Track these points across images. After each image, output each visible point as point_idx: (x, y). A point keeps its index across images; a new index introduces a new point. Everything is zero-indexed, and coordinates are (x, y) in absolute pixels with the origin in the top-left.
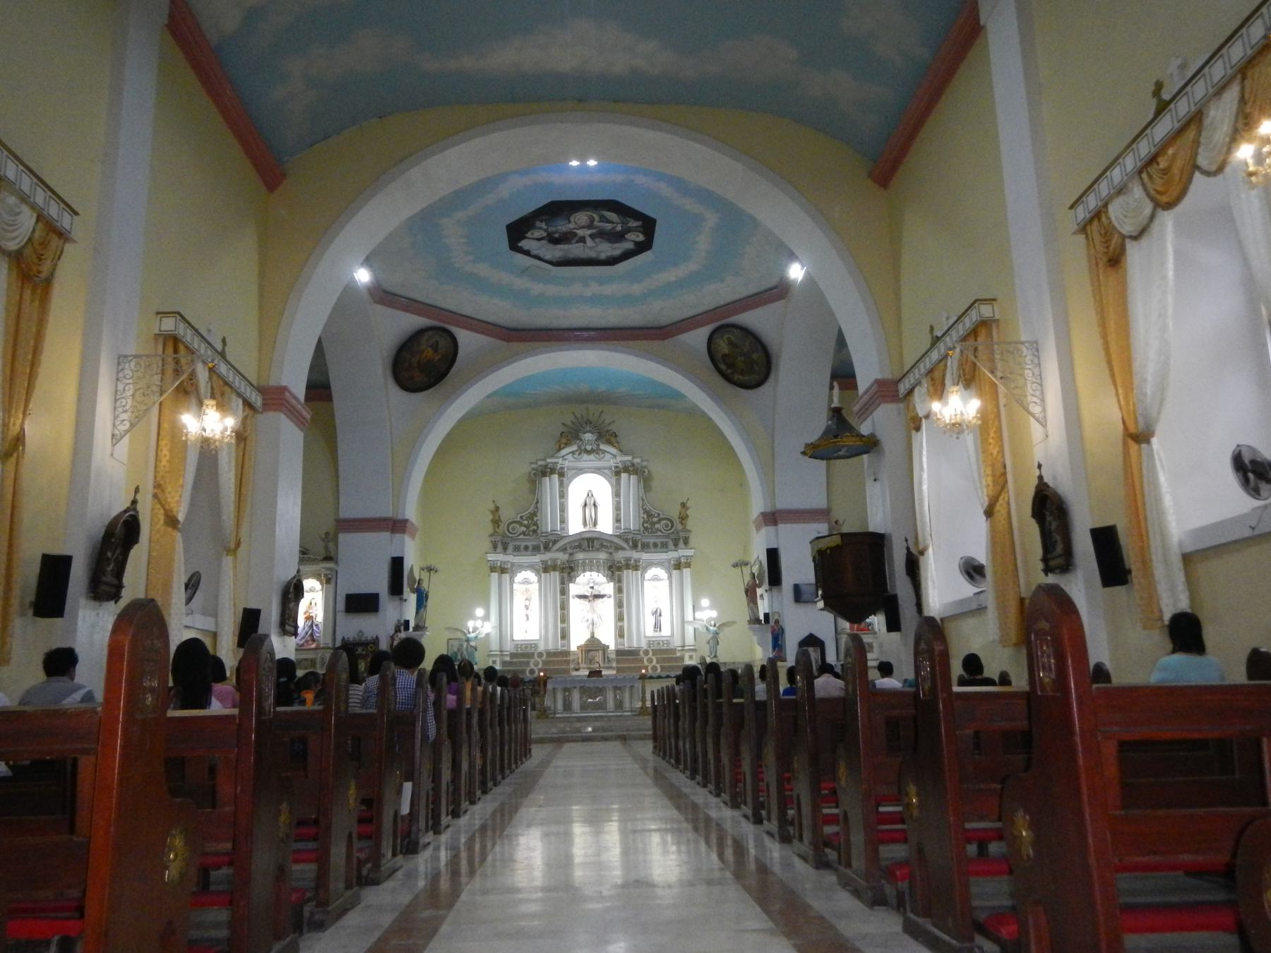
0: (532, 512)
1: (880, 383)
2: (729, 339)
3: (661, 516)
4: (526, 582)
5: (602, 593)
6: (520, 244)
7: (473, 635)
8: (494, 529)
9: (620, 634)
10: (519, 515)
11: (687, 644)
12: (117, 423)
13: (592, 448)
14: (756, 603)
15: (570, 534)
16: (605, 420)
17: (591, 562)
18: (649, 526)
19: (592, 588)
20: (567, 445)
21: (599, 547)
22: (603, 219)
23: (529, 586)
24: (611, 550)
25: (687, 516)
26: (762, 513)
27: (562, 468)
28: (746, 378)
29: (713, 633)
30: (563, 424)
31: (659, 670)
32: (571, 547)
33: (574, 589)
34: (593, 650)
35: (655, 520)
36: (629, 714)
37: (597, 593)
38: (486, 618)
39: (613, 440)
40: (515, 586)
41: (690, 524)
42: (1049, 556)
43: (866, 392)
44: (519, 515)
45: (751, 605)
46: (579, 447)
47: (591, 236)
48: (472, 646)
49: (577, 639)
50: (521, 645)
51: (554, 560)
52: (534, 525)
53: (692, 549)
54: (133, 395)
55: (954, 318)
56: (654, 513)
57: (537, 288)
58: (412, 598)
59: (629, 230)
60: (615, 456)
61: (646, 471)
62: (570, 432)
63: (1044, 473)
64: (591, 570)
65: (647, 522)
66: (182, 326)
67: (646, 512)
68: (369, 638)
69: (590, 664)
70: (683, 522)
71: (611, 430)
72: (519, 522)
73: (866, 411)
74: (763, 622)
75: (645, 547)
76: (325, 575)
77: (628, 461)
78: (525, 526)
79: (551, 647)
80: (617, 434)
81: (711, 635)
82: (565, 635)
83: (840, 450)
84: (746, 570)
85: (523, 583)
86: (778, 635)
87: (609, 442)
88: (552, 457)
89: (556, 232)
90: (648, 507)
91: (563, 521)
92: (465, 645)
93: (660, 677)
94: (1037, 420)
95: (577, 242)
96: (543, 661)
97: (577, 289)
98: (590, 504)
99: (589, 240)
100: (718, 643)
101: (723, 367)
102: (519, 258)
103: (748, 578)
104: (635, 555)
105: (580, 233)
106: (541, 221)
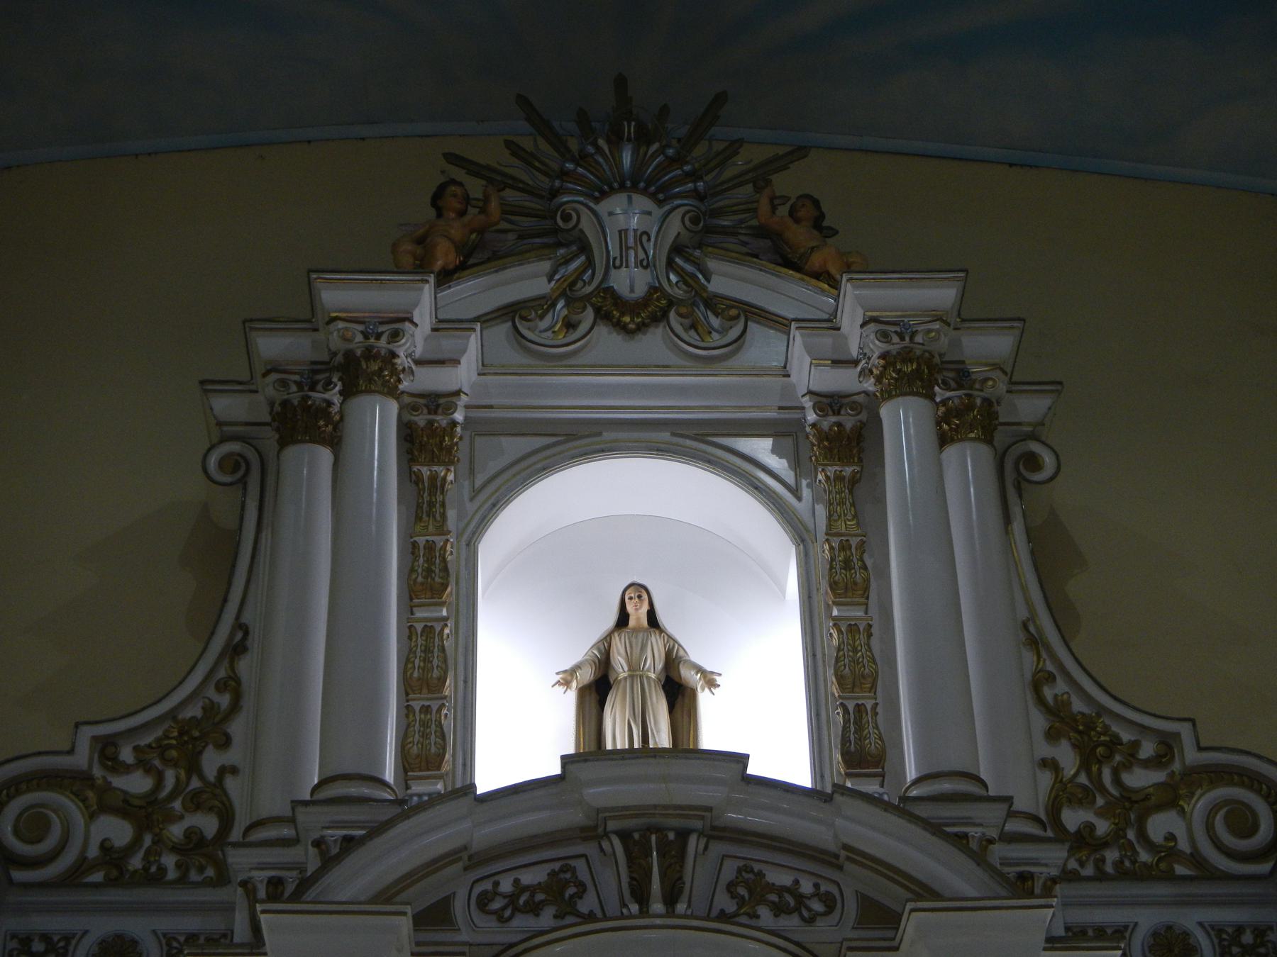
0: (194, 711)
3: (1192, 756)
13: (654, 289)
15: (487, 779)
21: (724, 902)
27: (438, 402)
30: (454, 159)
32: (483, 902)
35: (1139, 779)
39: (800, 235)
44: (87, 732)
52: (196, 803)
56: (1126, 736)
61: (1048, 459)
62: (509, 211)
65: (1083, 798)
71: (785, 199)
72: (85, 778)
78: (125, 807)
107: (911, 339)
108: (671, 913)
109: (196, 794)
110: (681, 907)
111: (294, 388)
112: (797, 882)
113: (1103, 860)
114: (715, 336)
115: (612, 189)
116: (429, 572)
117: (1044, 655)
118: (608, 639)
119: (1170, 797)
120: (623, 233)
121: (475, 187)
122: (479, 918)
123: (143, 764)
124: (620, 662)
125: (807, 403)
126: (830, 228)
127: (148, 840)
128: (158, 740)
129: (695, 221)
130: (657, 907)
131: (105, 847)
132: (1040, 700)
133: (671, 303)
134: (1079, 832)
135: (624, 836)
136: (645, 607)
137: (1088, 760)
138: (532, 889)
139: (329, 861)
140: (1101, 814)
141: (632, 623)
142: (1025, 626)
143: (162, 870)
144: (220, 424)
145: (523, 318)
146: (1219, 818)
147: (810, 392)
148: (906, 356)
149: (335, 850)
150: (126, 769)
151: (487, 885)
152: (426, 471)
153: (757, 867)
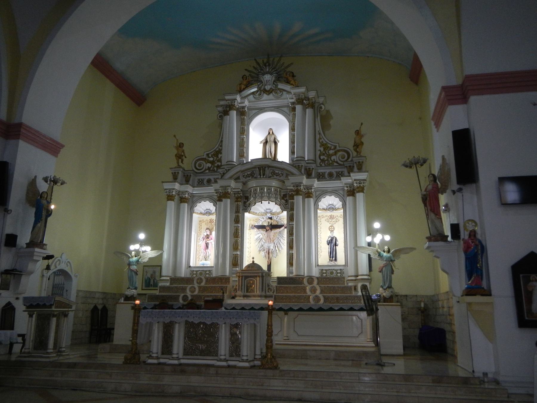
0: (217, 150)
3: (338, 148)
5: (280, 224)
7: (135, 259)
8: (178, 163)
11: (360, 274)
14: (438, 214)
16: (284, 63)
17: (262, 189)
18: (326, 158)
19: (271, 218)
20: (248, 85)
21: (270, 175)
24: (282, 178)
25: (362, 143)
26: (444, 88)
29: (385, 261)
30: (246, 70)
31: (322, 301)
32: (244, 176)
33: (249, 218)
34: (251, 277)
35: (331, 152)
36: (246, 364)
37: (274, 223)
39: (290, 78)
40: (195, 216)
41: (365, 150)
44: (205, 153)
45: (432, 215)
48: (132, 271)
50: (197, 271)
56: (329, 146)
60: (290, 93)
65: (324, 155)
67: (322, 145)
69: (247, 292)
70: (358, 149)
72: (206, 159)
74: (449, 239)
75: (320, 177)
77: (304, 93)
80: (294, 75)
81: (382, 263)
84: (423, 171)
85: (204, 214)
86: (476, 255)
93: (321, 309)
103: (426, 183)
107: (299, 96)
108: (263, 177)
109: (218, 160)
110: (264, 176)
111: (225, 108)
112: (279, 172)
113: (325, 163)
114: (279, 94)
115: (265, 74)
116: (242, 131)
117: (321, 135)
118: (267, 136)
119: (335, 154)
120: (266, 81)
121: (247, 74)
122: (243, 178)
123: (212, 157)
124: (268, 139)
125: (290, 104)
126: (295, 76)
127: (213, 166)
128: (214, 154)
129: (276, 77)
130: (262, 176)
131: (208, 167)
132: (319, 142)
133: (273, 90)
134: (323, 159)
135: (258, 168)
136: (272, 131)
137: (324, 149)
138: (249, 174)
139: (227, 172)
140: (325, 156)
141: (270, 134)
142: (319, 131)
143: (215, 170)
144: (219, 111)
145: (254, 94)
146: (340, 156)
147: (290, 102)
148: (299, 99)
149: (228, 170)
150: (210, 157)
151: (244, 174)
152: (242, 117)
153: (275, 171)
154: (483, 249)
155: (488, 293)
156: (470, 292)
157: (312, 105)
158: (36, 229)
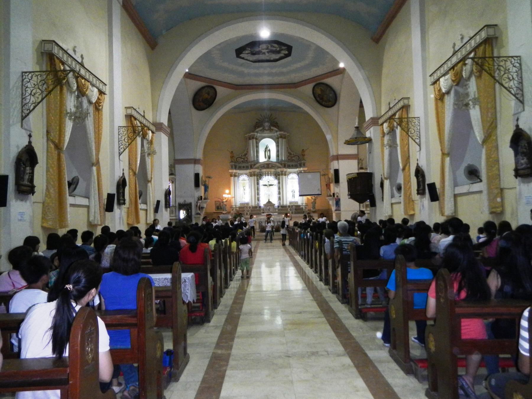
1: (372, 119)
2: (321, 88)
3: (295, 155)
4: (244, 180)
5: (272, 184)
6: (240, 56)
9: (279, 198)
10: (240, 155)
12: (120, 149)
19: (269, 182)
20: (259, 127)
22: (272, 46)
23: (245, 181)
25: (305, 155)
28: (327, 103)
33: (261, 182)
35: (292, 156)
37: (270, 184)
38: (230, 194)
42: (419, 189)
43: (368, 121)
45: (328, 190)
46: (263, 128)
47: (268, 52)
48: (225, 204)
49: (263, 202)
51: (254, 172)
53: (306, 167)
54: (124, 139)
55: (397, 101)
57: (246, 71)
58: (202, 188)
59: (282, 50)
63: (419, 163)
64: (268, 175)
66: (133, 111)
67: (289, 153)
68: (188, 203)
73: (368, 128)
75: (289, 167)
76: (172, 180)
78: (243, 158)
79: (253, 204)
81: (313, 201)
82: (258, 200)
83: (358, 142)
84: (326, 177)
87: (275, 126)
88: (253, 132)
89: (254, 51)
90: (290, 151)
91: (258, 156)
92: (222, 204)
94: (418, 144)
95: (262, 54)
96: (251, 210)
97: (261, 71)
98: (267, 150)
99: (267, 54)
100: (316, 203)
101: (318, 99)
102: (240, 61)
104: (285, 170)
105: (263, 51)
106: (249, 48)
154: (339, 200)
155: (340, 210)
156: (336, 210)
157: (285, 138)
158: (206, 194)
